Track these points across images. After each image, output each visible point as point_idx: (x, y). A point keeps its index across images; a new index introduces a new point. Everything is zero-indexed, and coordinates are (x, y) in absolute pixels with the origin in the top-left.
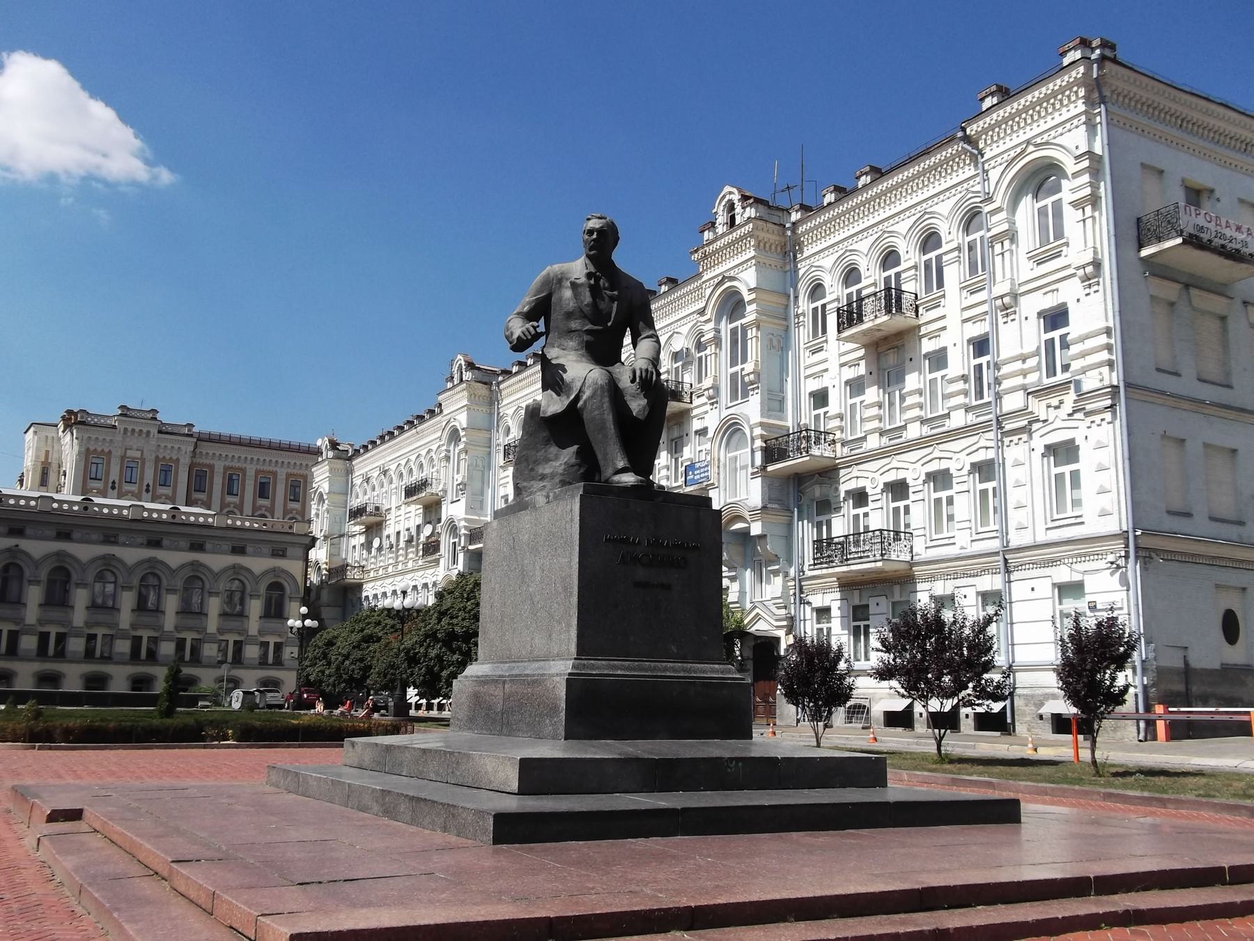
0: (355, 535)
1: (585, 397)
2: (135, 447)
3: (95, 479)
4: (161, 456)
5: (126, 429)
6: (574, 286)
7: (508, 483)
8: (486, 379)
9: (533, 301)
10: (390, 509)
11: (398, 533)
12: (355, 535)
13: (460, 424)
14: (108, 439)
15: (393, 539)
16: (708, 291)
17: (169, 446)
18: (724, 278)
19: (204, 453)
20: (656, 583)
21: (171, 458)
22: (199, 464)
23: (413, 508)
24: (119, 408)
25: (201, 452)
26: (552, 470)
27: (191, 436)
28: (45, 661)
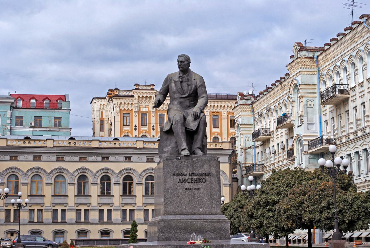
0: (258, 147)
3: (126, 125)
5: (139, 97)
6: (175, 82)
7: (327, 113)
8: (311, 55)
9: (163, 88)
10: (273, 131)
11: (278, 144)
12: (258, 147)
15: (276, 148)
23: (284, 130)
24: (134, 85)
26: (168, 149)
28: (103, 224)
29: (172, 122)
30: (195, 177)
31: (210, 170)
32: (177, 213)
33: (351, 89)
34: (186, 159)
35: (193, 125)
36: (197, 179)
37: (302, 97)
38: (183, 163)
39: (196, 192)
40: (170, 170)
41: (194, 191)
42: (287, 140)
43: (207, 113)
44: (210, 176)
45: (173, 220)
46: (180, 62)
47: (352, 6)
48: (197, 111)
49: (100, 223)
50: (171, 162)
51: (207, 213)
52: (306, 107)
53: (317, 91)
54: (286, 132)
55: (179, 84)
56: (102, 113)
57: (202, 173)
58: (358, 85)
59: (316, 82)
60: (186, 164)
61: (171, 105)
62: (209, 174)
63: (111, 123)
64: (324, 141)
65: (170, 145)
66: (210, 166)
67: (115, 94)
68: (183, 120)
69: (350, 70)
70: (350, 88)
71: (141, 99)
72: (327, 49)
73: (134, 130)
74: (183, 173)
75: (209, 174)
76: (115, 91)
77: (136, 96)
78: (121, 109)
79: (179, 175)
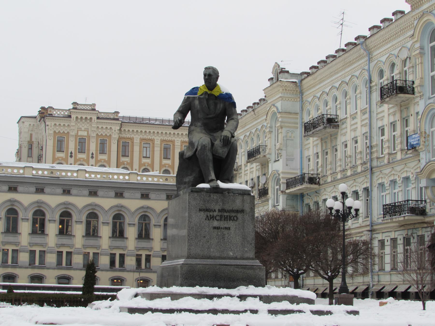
1: (198, 150)
2: (83, 129)
4: (100, 134)
5: (77, 118)
13: (277, 109)
14: (66, 125)
16: (416, 22)
17: (104, 127)
18: (423, 13)
19: (127, 130)
20: (223, 227)
21: (106, 135)
22: (124, 138)
23: (254, 165)
24: (72, 104)
25: (125, 130)
27: (117, 119)
29: (197, 147)
30: (225, 214)
31: (243, 206)
32: (203, 256)
33: (341, 120)
34: (215, 193)
35: (222, 152)
36: (227, 216)
37: (282, 128)
38: (212, 196)
39: (226, 232)
40: (197, 205)
41: (223, 230)
42: (258, 177)
43: (157, 141)
44: (242, 213)
45: (199, 264)
46: (207, 76)
47: (341, 25)
48: (228, 135)
49: (31, 266)
50: (198, 195)
51: (239, 257)
52: (285, 139)
53: (299, 121)
54: (258, 168)
55: (205, 102)
56: (31, 135)
57: (233, 209)
58: (349, 117)
59: (298, 109)
60: (215, 198)
61: (193, 128)
62: (242, 211)
63: (42, 147)
64: (306, 179)
65: (191, 175)
66: (243, 201)
67: (49, 113)
68: (210, 144)
69: (340, 98)
70: (339, 119)
71: (79, 120)
72: (313, 73)
73: (69, 158)
74: (211, 209)
75: (242, 211)
76: (49, 110)
77: (73, 116)
78: (55, 132)
79: (207, 210)
